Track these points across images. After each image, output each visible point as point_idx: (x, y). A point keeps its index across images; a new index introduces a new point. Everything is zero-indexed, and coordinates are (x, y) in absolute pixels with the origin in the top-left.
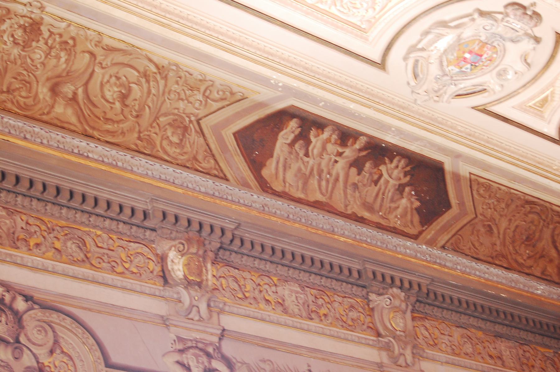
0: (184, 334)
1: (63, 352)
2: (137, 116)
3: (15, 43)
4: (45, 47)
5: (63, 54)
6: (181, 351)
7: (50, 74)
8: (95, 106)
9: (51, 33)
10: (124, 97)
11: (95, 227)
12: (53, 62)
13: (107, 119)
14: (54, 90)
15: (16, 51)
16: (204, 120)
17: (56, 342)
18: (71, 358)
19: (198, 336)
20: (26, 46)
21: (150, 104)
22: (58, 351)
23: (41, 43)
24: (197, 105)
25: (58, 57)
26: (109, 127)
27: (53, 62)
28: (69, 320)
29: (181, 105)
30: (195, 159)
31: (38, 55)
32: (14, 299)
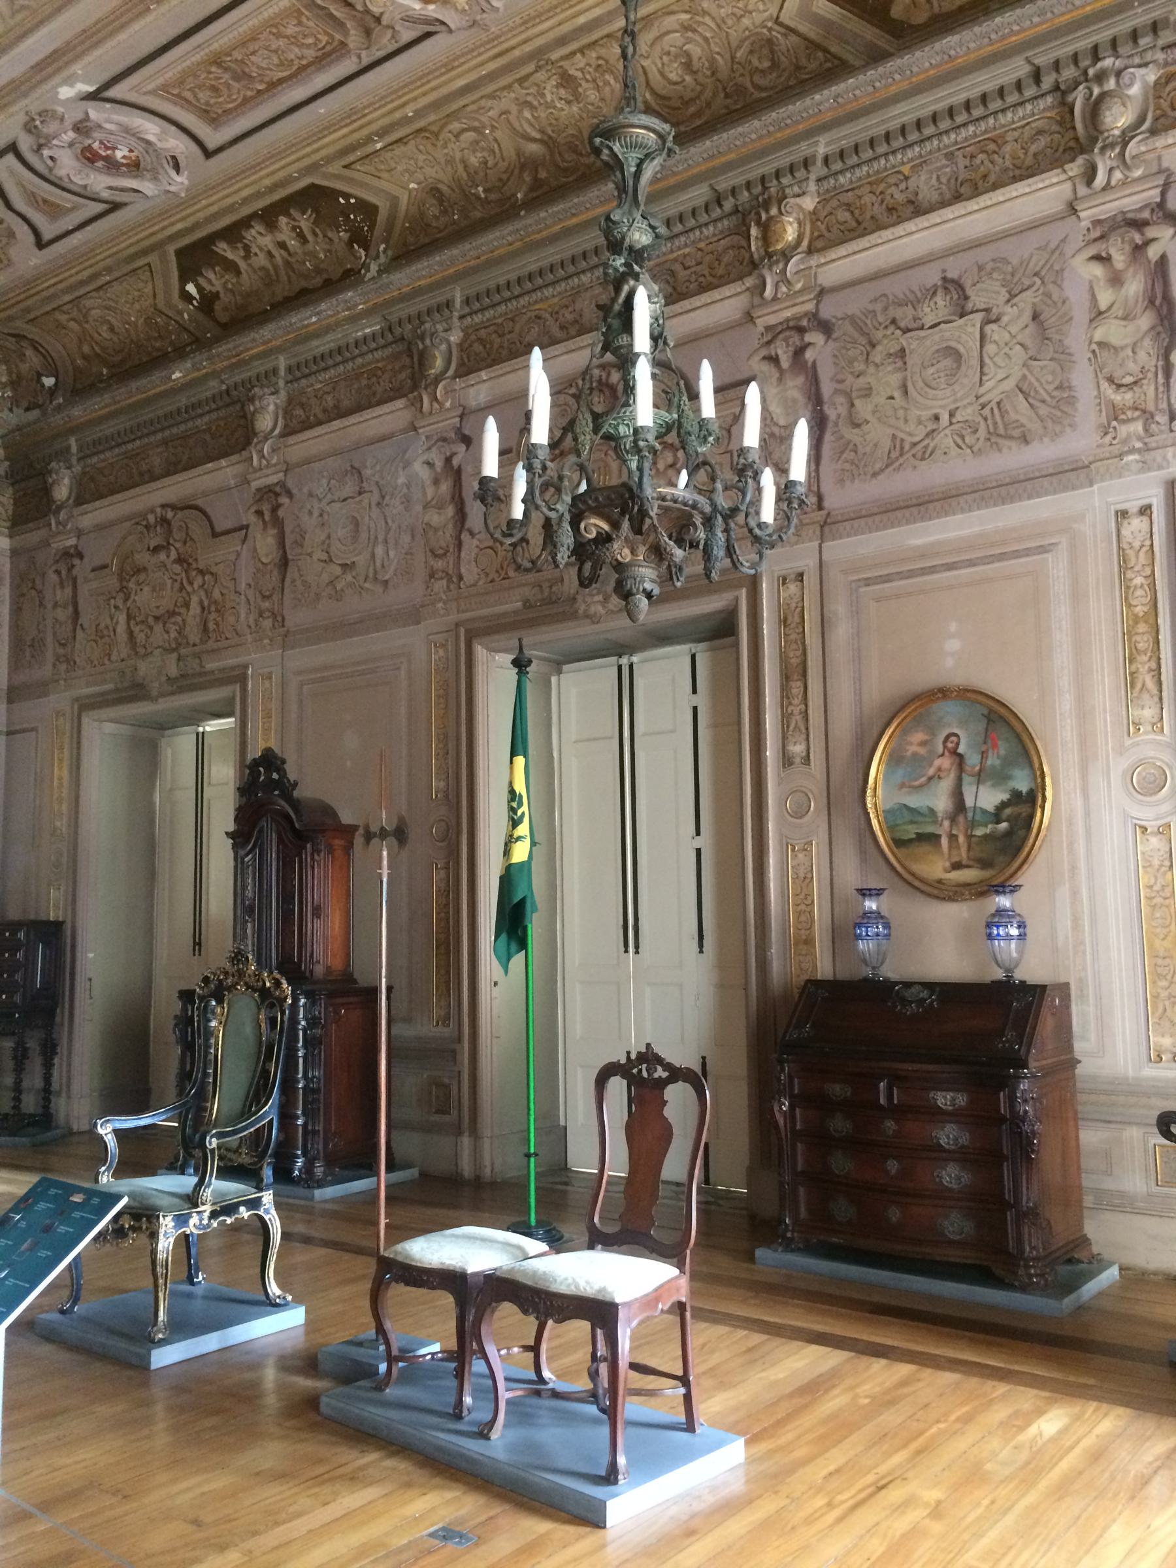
0: (772, 320)
2: (713, 74)
3: (569, 102)
4: (590, 85)
5: (607, 77)
6: (769, 343)
8: (669, 99)
9: (581, 70)
10: (688, 66)
11: (679, 248)
13: (687, 103)
16: (782, 15)
19: (788, 314)
20: (577, 97)
21: (717, 50)
23: (583, 83)
24: (761, 7)
25: (607, 83)
26: (692, 109)
27: (607, 89)
29: (746, 21)
30: (798, 68)
31: (593, 95)
32: (609, 374)
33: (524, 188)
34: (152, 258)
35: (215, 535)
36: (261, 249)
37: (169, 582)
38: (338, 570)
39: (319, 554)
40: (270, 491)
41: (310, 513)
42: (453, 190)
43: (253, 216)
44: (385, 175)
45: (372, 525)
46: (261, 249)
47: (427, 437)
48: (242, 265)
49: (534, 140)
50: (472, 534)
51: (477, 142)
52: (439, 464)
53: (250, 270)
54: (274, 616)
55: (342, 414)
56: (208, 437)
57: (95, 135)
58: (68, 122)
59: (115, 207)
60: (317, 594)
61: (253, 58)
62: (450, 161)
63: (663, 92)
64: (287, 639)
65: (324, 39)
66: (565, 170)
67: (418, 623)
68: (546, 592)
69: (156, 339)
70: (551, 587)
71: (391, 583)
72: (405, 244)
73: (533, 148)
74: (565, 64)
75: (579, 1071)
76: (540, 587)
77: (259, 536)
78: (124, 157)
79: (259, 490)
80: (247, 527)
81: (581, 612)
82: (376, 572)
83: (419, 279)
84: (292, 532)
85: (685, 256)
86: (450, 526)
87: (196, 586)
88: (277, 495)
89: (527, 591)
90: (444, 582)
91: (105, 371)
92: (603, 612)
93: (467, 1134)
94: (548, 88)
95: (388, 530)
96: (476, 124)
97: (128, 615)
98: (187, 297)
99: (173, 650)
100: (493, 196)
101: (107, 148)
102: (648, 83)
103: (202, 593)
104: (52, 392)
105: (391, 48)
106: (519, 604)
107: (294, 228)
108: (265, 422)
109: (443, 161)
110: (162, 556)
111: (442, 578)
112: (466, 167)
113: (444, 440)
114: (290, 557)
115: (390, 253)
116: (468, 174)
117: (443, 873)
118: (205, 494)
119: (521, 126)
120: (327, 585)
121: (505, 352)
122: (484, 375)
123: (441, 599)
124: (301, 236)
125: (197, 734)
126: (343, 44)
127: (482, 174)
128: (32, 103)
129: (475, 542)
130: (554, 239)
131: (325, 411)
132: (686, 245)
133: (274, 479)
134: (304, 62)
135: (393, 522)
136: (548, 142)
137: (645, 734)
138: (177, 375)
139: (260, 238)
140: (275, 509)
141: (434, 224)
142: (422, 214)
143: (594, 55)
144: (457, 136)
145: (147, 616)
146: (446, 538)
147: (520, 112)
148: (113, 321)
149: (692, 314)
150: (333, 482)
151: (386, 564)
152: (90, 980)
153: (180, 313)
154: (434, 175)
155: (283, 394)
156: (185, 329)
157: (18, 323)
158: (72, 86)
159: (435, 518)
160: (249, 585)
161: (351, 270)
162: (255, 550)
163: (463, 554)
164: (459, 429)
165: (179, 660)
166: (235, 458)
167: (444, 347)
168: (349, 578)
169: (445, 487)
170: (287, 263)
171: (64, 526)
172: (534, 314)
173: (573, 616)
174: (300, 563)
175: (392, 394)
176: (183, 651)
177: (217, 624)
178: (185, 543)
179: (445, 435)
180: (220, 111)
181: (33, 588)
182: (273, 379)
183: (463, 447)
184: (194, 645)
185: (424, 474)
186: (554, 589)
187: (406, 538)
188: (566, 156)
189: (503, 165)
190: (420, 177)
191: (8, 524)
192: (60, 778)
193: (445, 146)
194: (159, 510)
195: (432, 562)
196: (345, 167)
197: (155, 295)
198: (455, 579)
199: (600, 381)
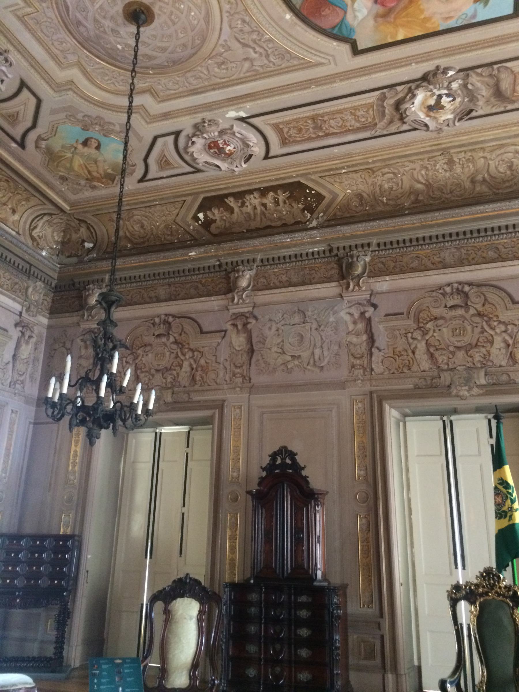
1: (489, 303)
3: (446, 171)
4: (460, 166)
5: (470, 164)
7: (467, 176)
8: (496, 178)
9: (460, 159)
10: (510, 167)
11: (502, 239)
12: (467, 170)
14: (473, 181)
15: (448, 174)
17: (486, 300)
18: (494, 305)
22: (487, 304)
23: (457, 165)
26: (507, 184)
27: (467, 169)
28: (492, 288)
32: (463, 287)
33: (409, 202)
34: (189, 199)
35: (202, 332)
36: (251, 204)
37: (168, 354)
38: (289, 358)
39: (275, 349)
40: (243, 315)
41: (270, 328)
42: (369, 197)
43: (258, 189)
44: (338, 184)
45: (312, 339)
46: (251, 204)
47: (348, 301)
48: (236, 210)
49: (421, 183)
50: (380, 350)
51: (392, 179)
52: (357, 315)
53: (239, 213)
54: (244, 377)
55: (291, 285)
56: (200, 286)
57: (225, 137)
58: (220, 128)
59: (198, 171)
60: (273, 368)
61: (331, 121)
62: (374, 184)
63: (493, 175)
64: (252, 389)
65: (370, 120)
66: (435, 198)
67: (344, 389)
68: (429, 382)
69: (168, 235)
70: (432, 380)
71: (325, 368)
72: (335, 215)
73: (419, 186)
74: (454, 155)
75: (428, 633)
76: (425, 379)
77: (234, 336)
78: (229, 150)
79: (234, 314)
80: (226, 331)
81: (454, 392)
82: (315, 361)
83: (357, 231)
84: (257, 337)
85: (505, 243)
86: (365, 344)
87: (187, 357)
88: (247, 318)
89: (416, 380)
90: (362, 371)
91: (129, 246)
92: (468, 395)
93: (389, 672)
94: (440, 163)
95: (323, 342)
96: (396, 171)
97: (136, 366)
98: (197, 219)
99: (169, 388)
100: (391, 202)
101: (225, 144)
102: (488, 170)
103: (192, 361)
104: (89, 251)
105: (396, 131)
106: (412, 386)
107: (275, 198)
108: (243, 283)
109: (370, 183)
110: (164, 339)
111: (360, 369)
112: (380, 189)
113: (360, 304)
114: (255, 348)
115: (325, 218)
116: (380, 191)
117: (364, 521)
118: (197, 312)
119: (418, 176)
120: (281, 364)
121: (397, 270)
122: (387, 278)
123: (359, 379)
124: (277, 203)
125: (156, 433)
126: (376, 124)
127: (388, 193)
128: (208, 115)
129: (381, 354)
130: (439, 225)
131: (280, 282)
132: (506, 238)
133: (246, 310)
134: (350, 128)
135: (326, 338)
136: (428, 185)
137: (461, 456)
138: (193, 253)
139: (254, 200)
140: (245, 325)
141: (354, 209)
142: (348, 204)
143: (470, 154)
144: (383, 175)
145: (150, 369)
146: (364, 349)
147: (420, 170)
148: (145, 223)
149: (512, 268)
150: (285, 315)
151: (322, 358)
152: (87, 571)
153: (189, 226)
154: (363, 189)
155: (254, 271)
156: (189, 233)
157: (89, 215)
158: (237, 112)
159: (354, 339)
160: (227, 360)
161: (300, 221)
162: (231, 343)
163: (373, 359)
164: (370, 300)
165: (173, 393)
166: (220, 297)
167: (362, 262)
168: (296, 362)
169: (361, 326)
170: (263, 213)
171: (93, 317)
172: (415, 255)
173: (449, 395)
174: (262, 352)
175: (325, 280)
176: (176, 389)
177: (202, 378)
178: (181, 334)
179: (360, 302)
180: (291, 140)
181: (64, 346)
182: (252, 264)
183: (373, 309)
184: (184, 387)
185: (347, 318)
186: (434, 381)
187: (336, 348)
188: (436, 192)
189: (400, 191)
190: (355, 188)
191: (48, 312)
192: (76, 452)
193: (375, 177)
194: (163, 316)
195: (352, 360)
196: (320, 177)
197: (177, 215)
198: (368, 370)
199: (458, 289)
